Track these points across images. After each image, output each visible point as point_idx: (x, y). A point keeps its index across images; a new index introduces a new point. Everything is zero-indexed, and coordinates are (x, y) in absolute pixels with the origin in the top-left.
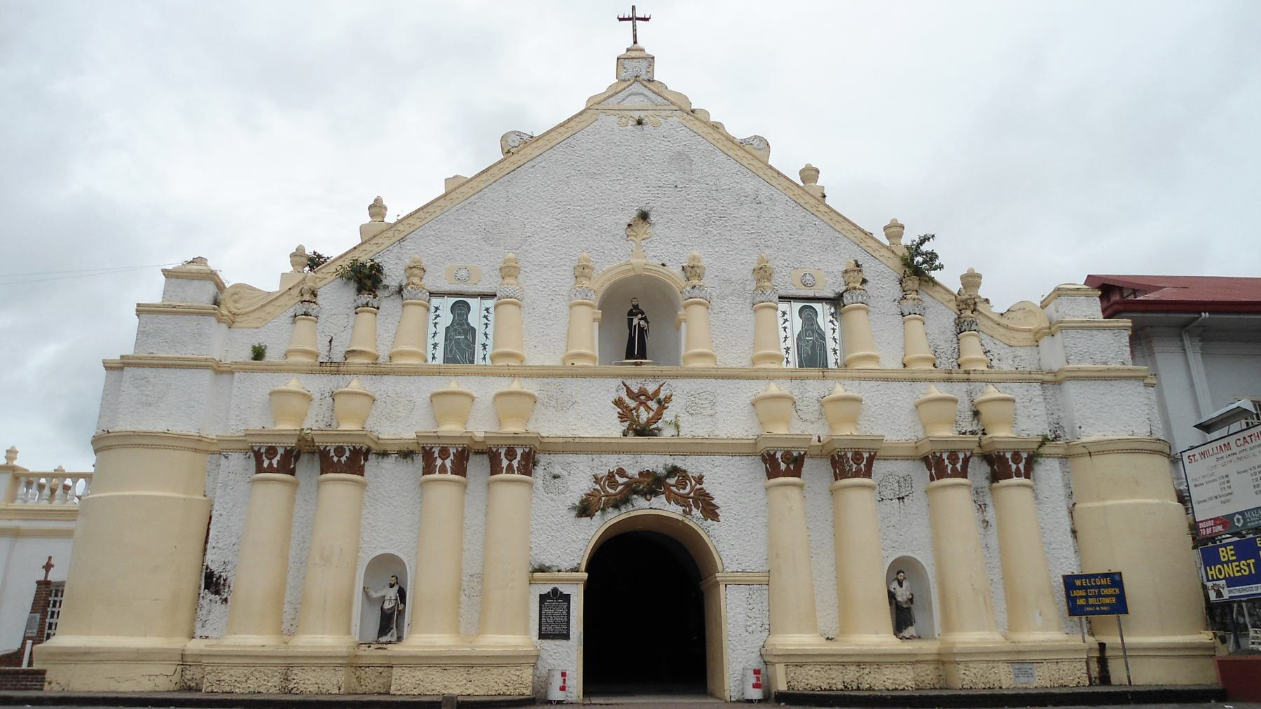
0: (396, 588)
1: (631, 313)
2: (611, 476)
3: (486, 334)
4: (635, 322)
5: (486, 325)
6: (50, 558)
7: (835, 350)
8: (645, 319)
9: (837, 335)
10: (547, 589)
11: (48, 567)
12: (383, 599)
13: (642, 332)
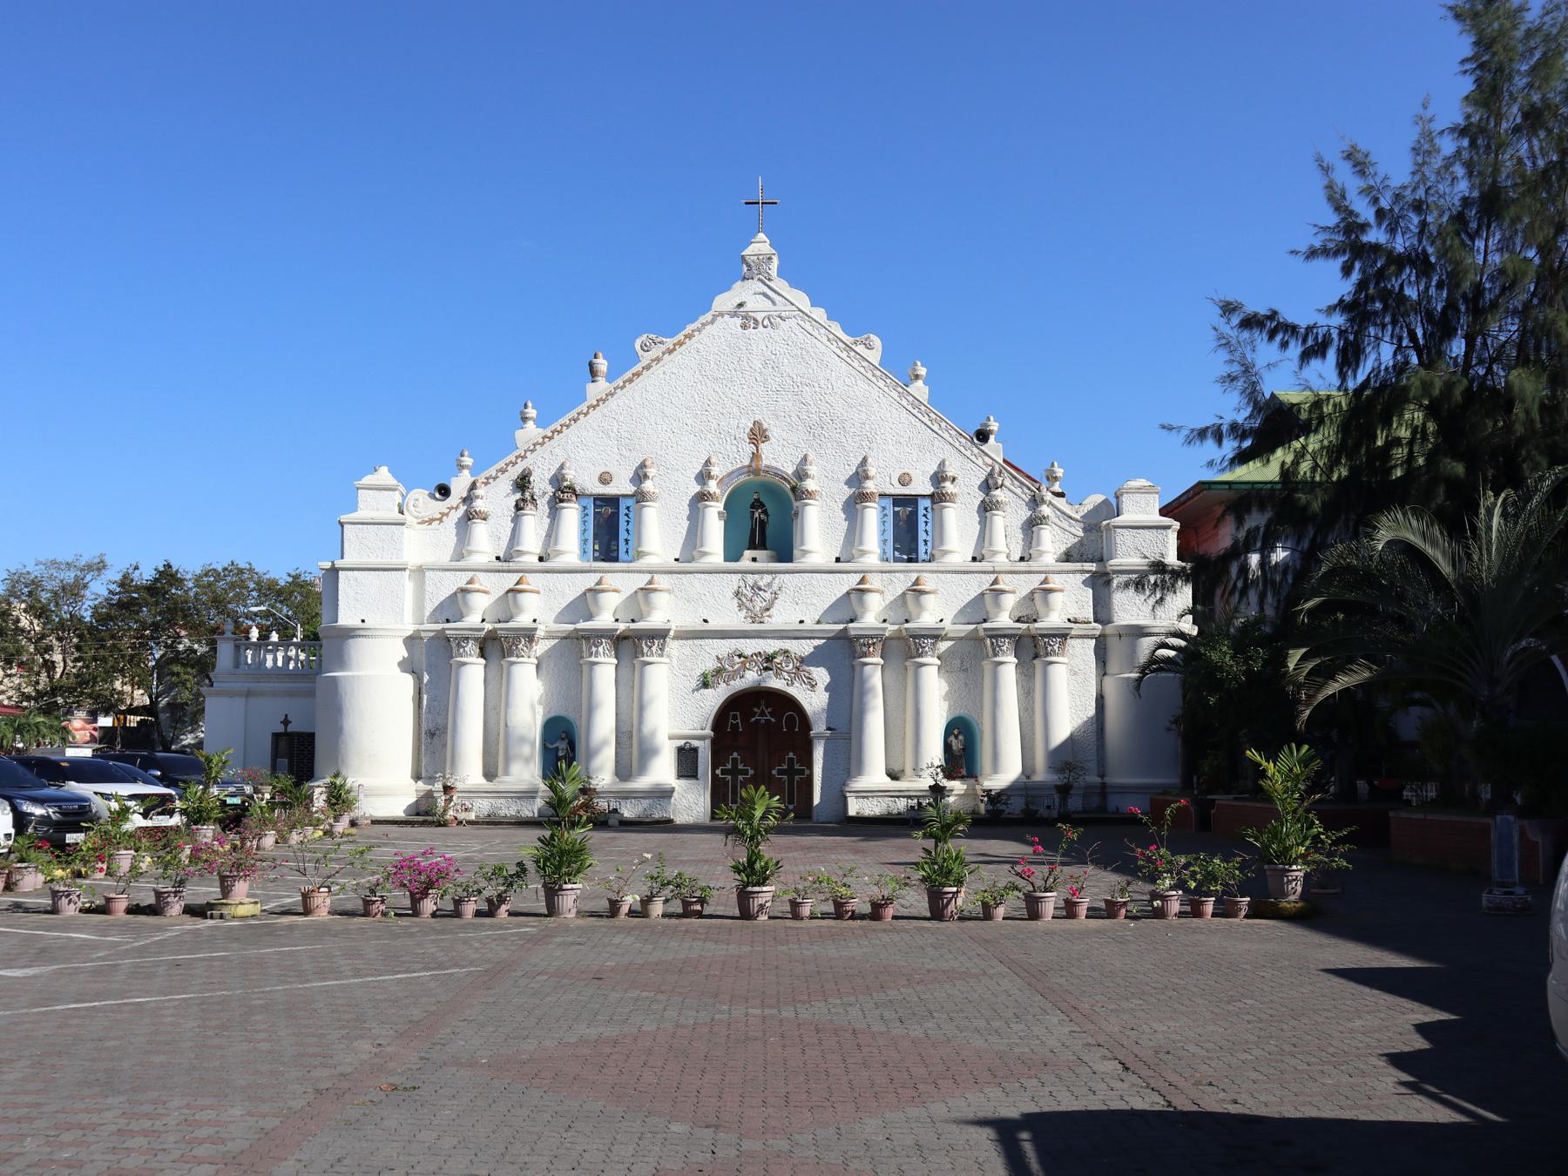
0: (566, 741)
1: (753, 506)
2: (730, 656)
3: (627, 530)
4: (757, 515)
5: (628, 522)
6: (286, 716)
7: (925, 541)
8: (765, 512)
9: (929, 528)
10: (681, 743)
11: (286, 722)
12: (557, 749)
13: (763, 524)
